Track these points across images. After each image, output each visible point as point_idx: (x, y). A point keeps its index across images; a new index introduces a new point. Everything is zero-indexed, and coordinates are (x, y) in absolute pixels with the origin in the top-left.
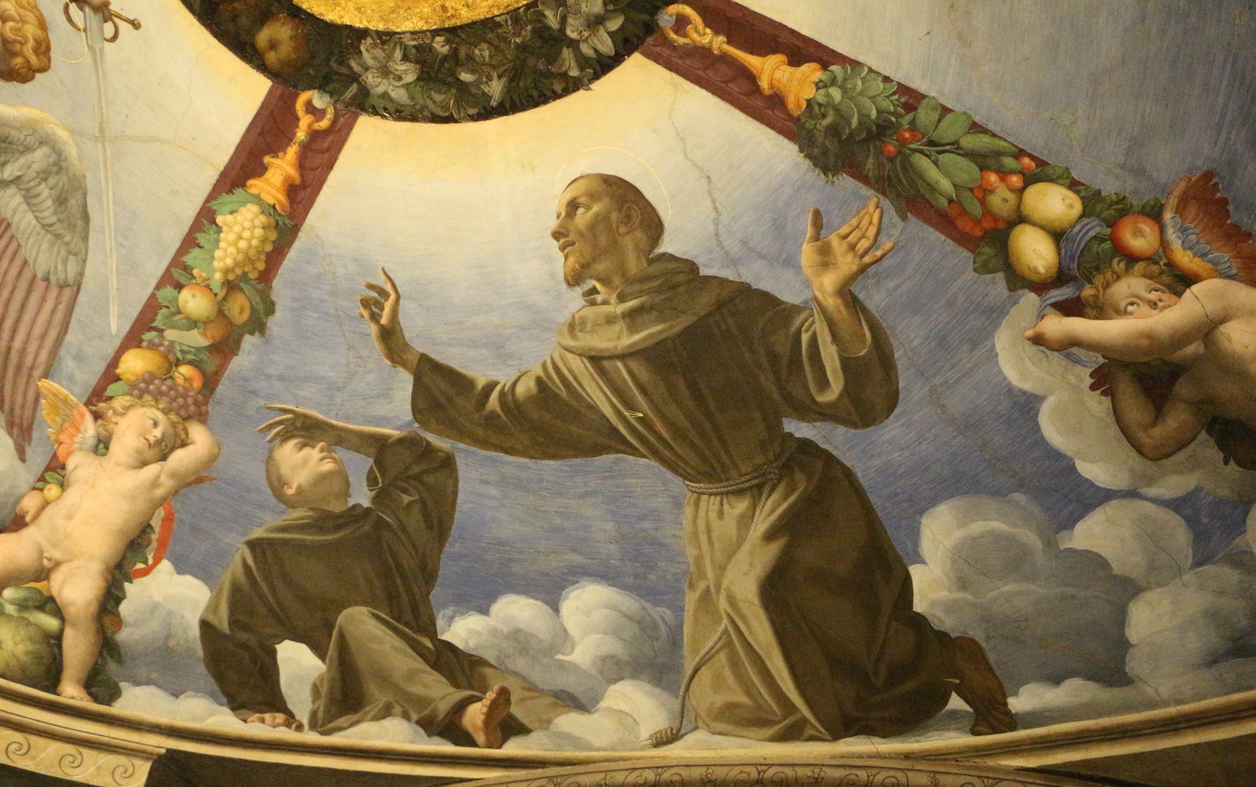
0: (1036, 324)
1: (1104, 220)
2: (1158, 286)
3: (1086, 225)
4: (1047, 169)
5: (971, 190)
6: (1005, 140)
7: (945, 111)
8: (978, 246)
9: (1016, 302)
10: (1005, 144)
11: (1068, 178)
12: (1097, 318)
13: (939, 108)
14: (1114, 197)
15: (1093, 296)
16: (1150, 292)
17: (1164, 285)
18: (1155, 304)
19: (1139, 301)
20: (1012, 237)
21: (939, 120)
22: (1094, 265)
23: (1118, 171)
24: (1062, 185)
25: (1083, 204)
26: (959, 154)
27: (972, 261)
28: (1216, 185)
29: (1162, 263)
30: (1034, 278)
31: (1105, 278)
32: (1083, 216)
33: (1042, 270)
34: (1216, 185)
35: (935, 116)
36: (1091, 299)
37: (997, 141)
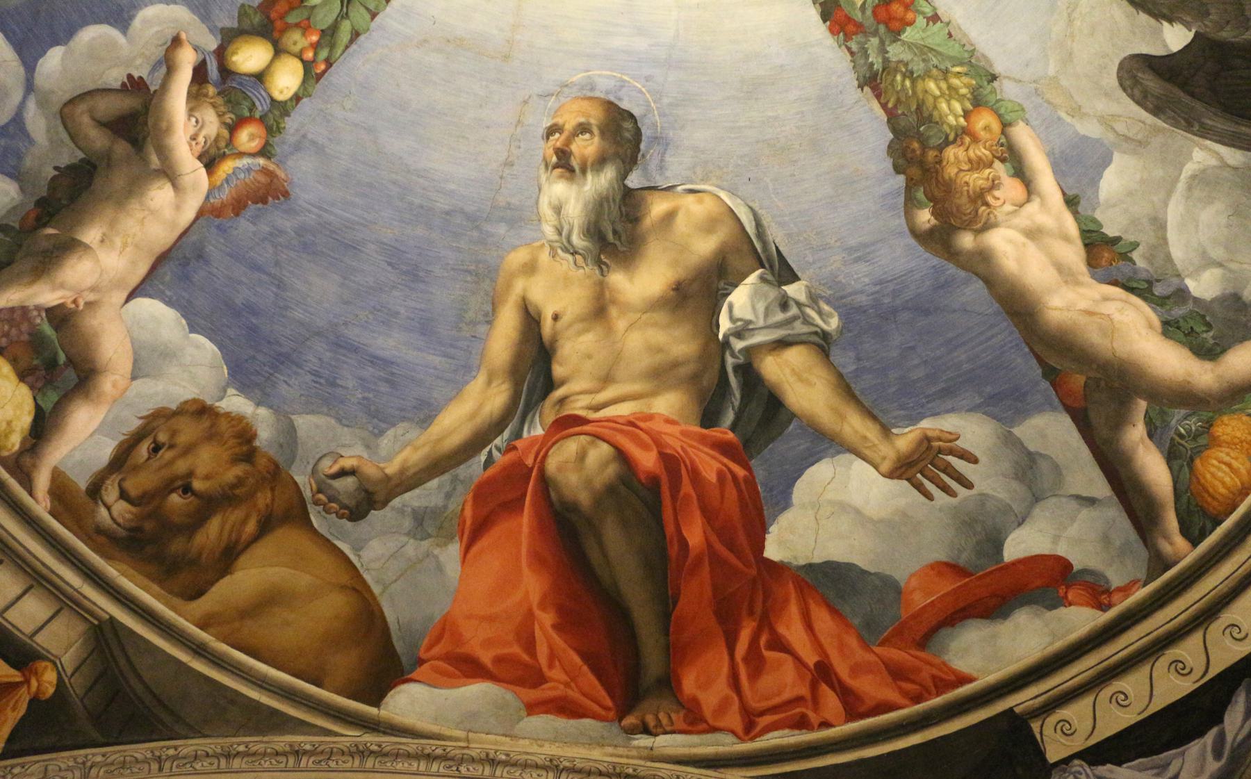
0: (190, 44)
1: (266, 115)
2: (208, 144)
3: (265, 100)
4: (313, 81)
5: (308, 19)
6: (341, 55)
7: (374, 16)
8: (263, 12)
9: (211, 31)
10: (338, 55)
11: (303, 95)
12: (188, 93)
13: (376, 11)
14: (283, 126)
15: (208, 93)
16: (205, 137)
17: (209, 148)
18: (194, 139)
19: (198, 127)
20: (264, 41)
21: (367, 9)
22: (232, 99)
23: (302, 132)
24: (299, 89)
25: (282, 102)
26: (338, 16)
27: (251, 4)
28: (278, 199)
29: (226, 150)
30: (230, 49)
31: (221, 105)
32: (273, 100)
33: (235, 58)
34: (278, 199)
35: (372, 7)
36: (205, 91)
37: (342, 48)
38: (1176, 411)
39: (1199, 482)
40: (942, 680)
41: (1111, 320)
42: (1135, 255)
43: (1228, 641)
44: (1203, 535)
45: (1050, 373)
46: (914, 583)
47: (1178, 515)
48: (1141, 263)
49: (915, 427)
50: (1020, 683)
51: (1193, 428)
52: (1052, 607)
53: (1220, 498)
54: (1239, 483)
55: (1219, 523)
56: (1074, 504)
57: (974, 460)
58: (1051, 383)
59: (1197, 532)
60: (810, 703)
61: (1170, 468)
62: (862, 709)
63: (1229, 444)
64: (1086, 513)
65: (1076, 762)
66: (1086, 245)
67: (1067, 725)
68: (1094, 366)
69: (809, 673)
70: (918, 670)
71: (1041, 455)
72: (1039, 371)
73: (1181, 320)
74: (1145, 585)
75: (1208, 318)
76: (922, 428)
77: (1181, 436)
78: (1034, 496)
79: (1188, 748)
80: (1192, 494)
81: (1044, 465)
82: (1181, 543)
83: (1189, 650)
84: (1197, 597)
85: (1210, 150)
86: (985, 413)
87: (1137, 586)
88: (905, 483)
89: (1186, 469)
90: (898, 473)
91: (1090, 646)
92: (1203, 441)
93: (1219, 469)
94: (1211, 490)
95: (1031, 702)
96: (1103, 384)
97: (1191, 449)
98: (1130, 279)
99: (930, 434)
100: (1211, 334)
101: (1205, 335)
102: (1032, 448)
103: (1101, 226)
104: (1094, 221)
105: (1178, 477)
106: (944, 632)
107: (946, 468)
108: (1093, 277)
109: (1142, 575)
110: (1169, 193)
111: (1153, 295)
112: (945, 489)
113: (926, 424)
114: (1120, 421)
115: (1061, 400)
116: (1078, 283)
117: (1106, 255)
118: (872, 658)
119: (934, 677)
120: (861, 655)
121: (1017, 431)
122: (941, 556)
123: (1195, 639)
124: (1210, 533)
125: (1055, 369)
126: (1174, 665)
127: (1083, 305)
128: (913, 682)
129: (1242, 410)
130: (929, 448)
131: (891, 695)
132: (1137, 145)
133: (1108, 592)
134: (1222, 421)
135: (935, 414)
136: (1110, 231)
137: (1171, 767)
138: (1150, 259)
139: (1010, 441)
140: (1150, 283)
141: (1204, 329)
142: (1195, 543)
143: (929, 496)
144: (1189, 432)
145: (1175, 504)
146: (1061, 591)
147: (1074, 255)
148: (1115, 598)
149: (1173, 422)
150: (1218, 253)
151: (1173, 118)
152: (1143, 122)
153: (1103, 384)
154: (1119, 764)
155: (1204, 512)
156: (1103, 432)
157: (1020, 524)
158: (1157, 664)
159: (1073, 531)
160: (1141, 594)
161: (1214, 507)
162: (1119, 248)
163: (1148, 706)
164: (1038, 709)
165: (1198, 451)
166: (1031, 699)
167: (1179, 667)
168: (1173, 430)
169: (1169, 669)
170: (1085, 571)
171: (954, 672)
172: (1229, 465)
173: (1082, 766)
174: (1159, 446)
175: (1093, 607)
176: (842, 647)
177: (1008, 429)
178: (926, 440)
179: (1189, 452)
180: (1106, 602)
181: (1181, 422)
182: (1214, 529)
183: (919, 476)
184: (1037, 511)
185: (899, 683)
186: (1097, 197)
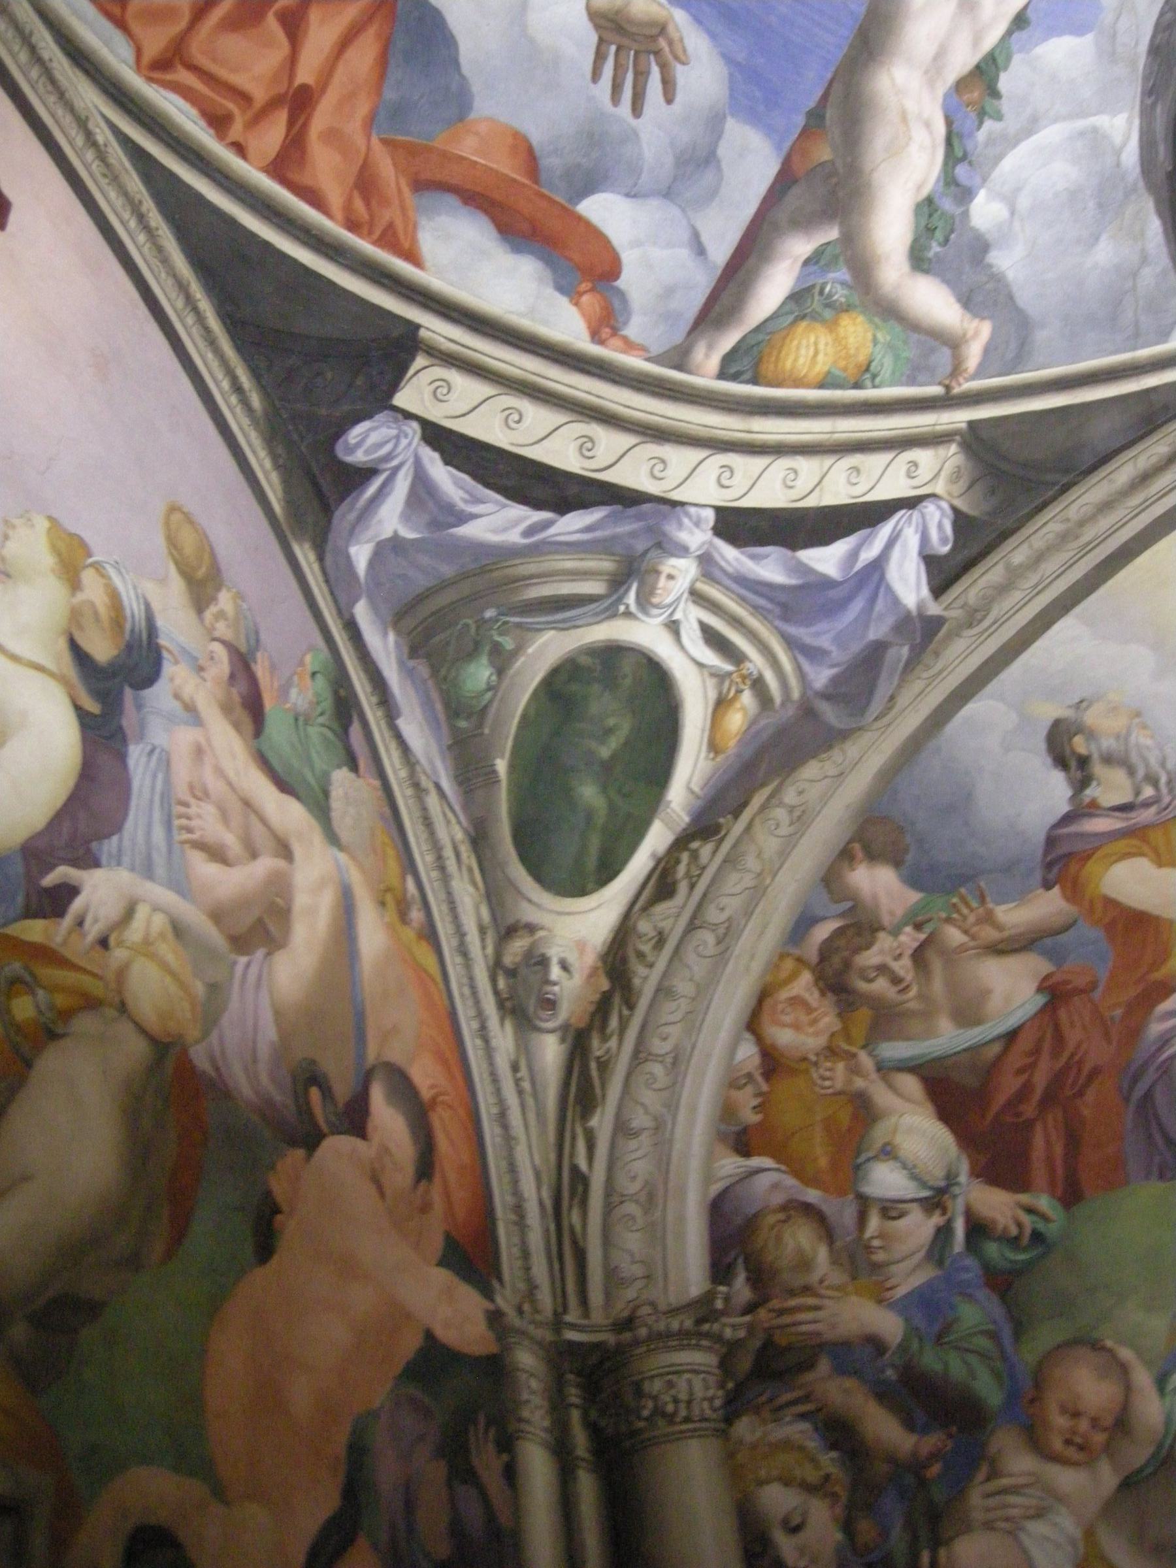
38: (844, 270)
39: (785, 338)
40: (395, 234)
41: (907, 144)
42: (988, 124)
43: (645, 469)
44: (735, 377)
45: (816, 117)
46: (483, 128)
47: (739, 342)
48: (981, 135)
49: (668, 6)
50: (455, 315)
51: (835, 298)
52: (560, 289)
53: (780, 367)
54: (805, 371)
55: (755, 381)
56: (685, 235)
57: (669, 98)
58: (805, 126)
59: (733, 370)
60: (250, 114)
61: (784, 303)
62: (291, 175)
63: (837, 340)
64: (684, 254)
65: (415, 425)
66: (978, 67)
67: (445, 391)
68: (849, 159)
69: (286, 85)
70: (385, 202)
71: (719, 169)
72: (812, 103)
73: (939, 212)
74: (648, 360)
75: (953, 236)
76: (672, 17)
77: (821, 292)
78: (669, 188)
79: (512, 507)
80: (769, 340)
81: (709, 177)
82: (713, 363)
83: (609, 442)
84: (670, 414)
85: (1130, 129)
86: (731, 75)
87: (641, 353)
88: (593, 38)
89: (791, 318)
90: (602, 22)
91: (546, 353)
92: (828, 314)
93: (808, 346)
94: (783, 353)
95: (442, 340)
96: (834, 180)
97: (813, 310)
98: (961, 136)
99: (671, 29)
100: (938, 249)
101: (934, 244)
102: (721, 152)
103: (1006, 68)
104: (1009, 59)
105: (778, 316)
106: (452, 200)
107: (642, 73)
108: (946, 96)
109: (656, 350)
110: (1070, 117)
111: (954, 167)
112: (617, 88)
113: (680, 17)
114: (803, 223)
115: (792, 148)
116: (931, 84)
117: (976, 94)
118: (360, 141)
119: (391, 226)
120: (354, 128)
121: (731, 125)
122: (536, 136)
123: (625, 440)
124: (741, 382)
125: (822, 117)
126: (585, 440)
127: (911, 105)
128: (368, 204)
129: (877, 327)
130: (653, 38)
131: (335, 196)
132: (1109, 53)
133: (615, 331)
134: (856, 318)
135: (698, 20)
136: (1004, 83)
137: (482, 506)
138: (991, 141)
139: (715, 124)
140: (965, 157)
141: (941, 239)
142: (722, 375)
143: (596, 75)
144: (830, 295)
145: (750, 332)
146: (583, 285)
147: (962, 60)
148: (615, 342)
149: (832, 275)
150: (1024, 202)
151: (1151, 73)
152: (1137, 44)
153: (834, 180)
154: (447, 462)
155: (757, 364)
156: (781, 214)
157: (627, 195)
158: (574, 424)
159: (657, 253)
160: (635, 362)
161: (768, 368)
162: (990, 104)
163: (524, 446)
164: (441, 352)
165: (815, 317)
166: (446, 338)
167: (586, 446)
168: (824, 281)
169: (577, 438)
170: (621, 294)
171: (414, 240)
172: (816, 353)
173: (415, 432)
174: (799, 279)
175: (589, 328)
176: (348, 98)
177: (727, 111)
178: (661, 29)
179: (809, 310)
180: (604, 336)
181: (836, 283)
182: (747, 382)
183: (613, 48)
184: (655, 203)
185: (356, 194)
186: (1036, 45)
